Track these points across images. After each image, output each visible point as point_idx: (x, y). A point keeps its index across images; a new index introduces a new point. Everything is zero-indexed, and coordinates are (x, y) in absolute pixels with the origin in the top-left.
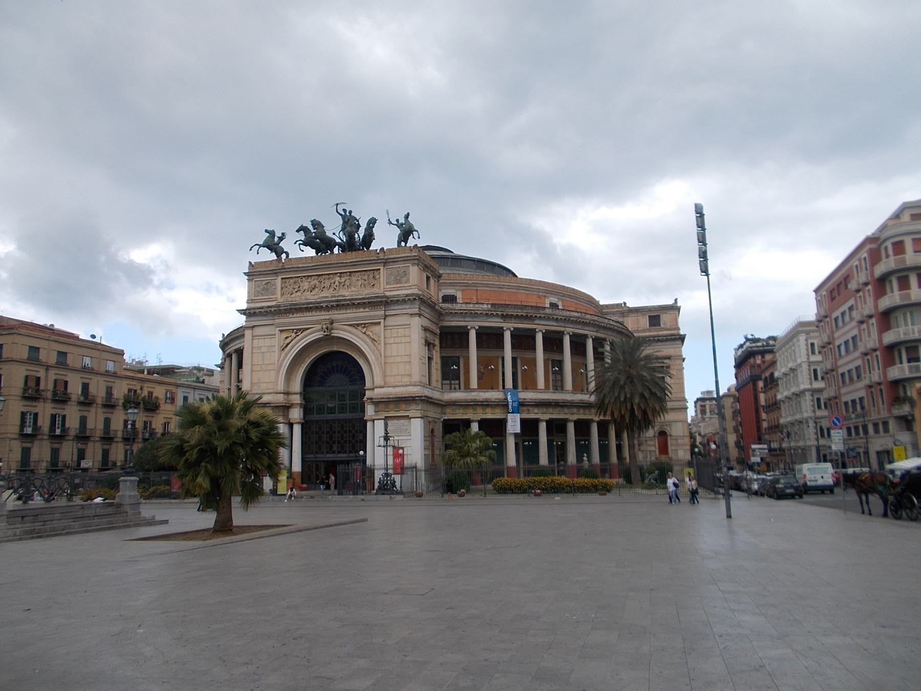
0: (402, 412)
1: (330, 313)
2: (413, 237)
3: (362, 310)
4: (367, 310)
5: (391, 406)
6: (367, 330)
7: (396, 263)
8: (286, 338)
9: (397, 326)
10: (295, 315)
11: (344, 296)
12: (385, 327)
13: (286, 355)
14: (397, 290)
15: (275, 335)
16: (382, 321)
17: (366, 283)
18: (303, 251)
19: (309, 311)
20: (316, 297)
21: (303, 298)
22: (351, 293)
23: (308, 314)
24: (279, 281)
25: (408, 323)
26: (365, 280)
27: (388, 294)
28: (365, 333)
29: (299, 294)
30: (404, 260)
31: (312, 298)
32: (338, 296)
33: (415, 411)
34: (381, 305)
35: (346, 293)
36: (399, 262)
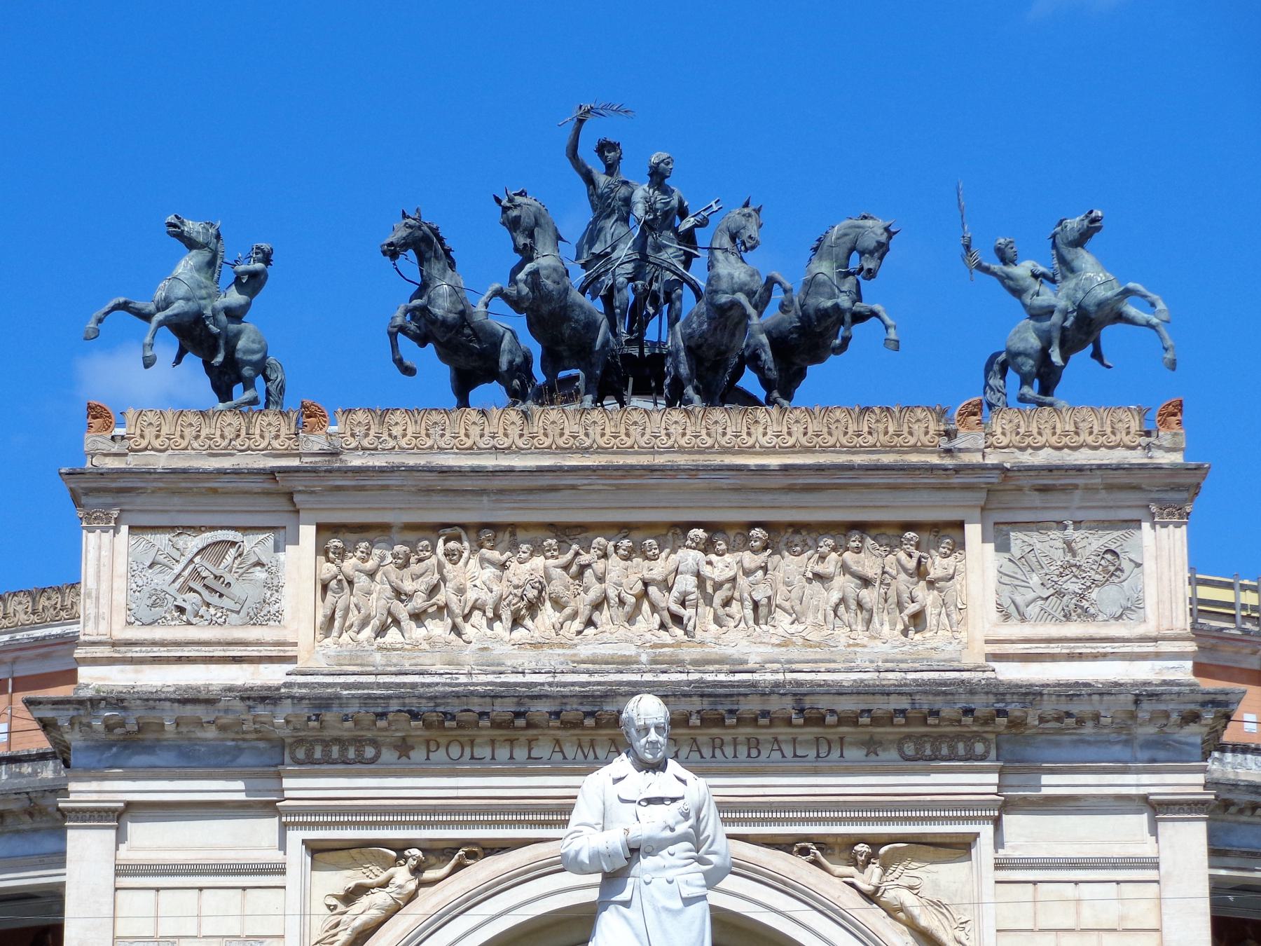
2: (1097, 355)
3: (853, 753)
7: (1055, 499)
8: (351, 896)
10: (418, 755)
11: (737, 665)
12: (999, 866)
14: (1071, 657)
15: (280, 870)
16: (986, 831)
17: (868, 595)
18: (408, 371)
19: (512, 742)
20: (552, 658)
21: (468, 655)
22: (782, 653)
25: (1146, 849)
26: (866, 582)
27: (1010, 673)
29: (437, 629)
30: (1110, 488)
31: (526, 659)
32: (695, 663)
34: (978, 736)
36: (1078, 494)
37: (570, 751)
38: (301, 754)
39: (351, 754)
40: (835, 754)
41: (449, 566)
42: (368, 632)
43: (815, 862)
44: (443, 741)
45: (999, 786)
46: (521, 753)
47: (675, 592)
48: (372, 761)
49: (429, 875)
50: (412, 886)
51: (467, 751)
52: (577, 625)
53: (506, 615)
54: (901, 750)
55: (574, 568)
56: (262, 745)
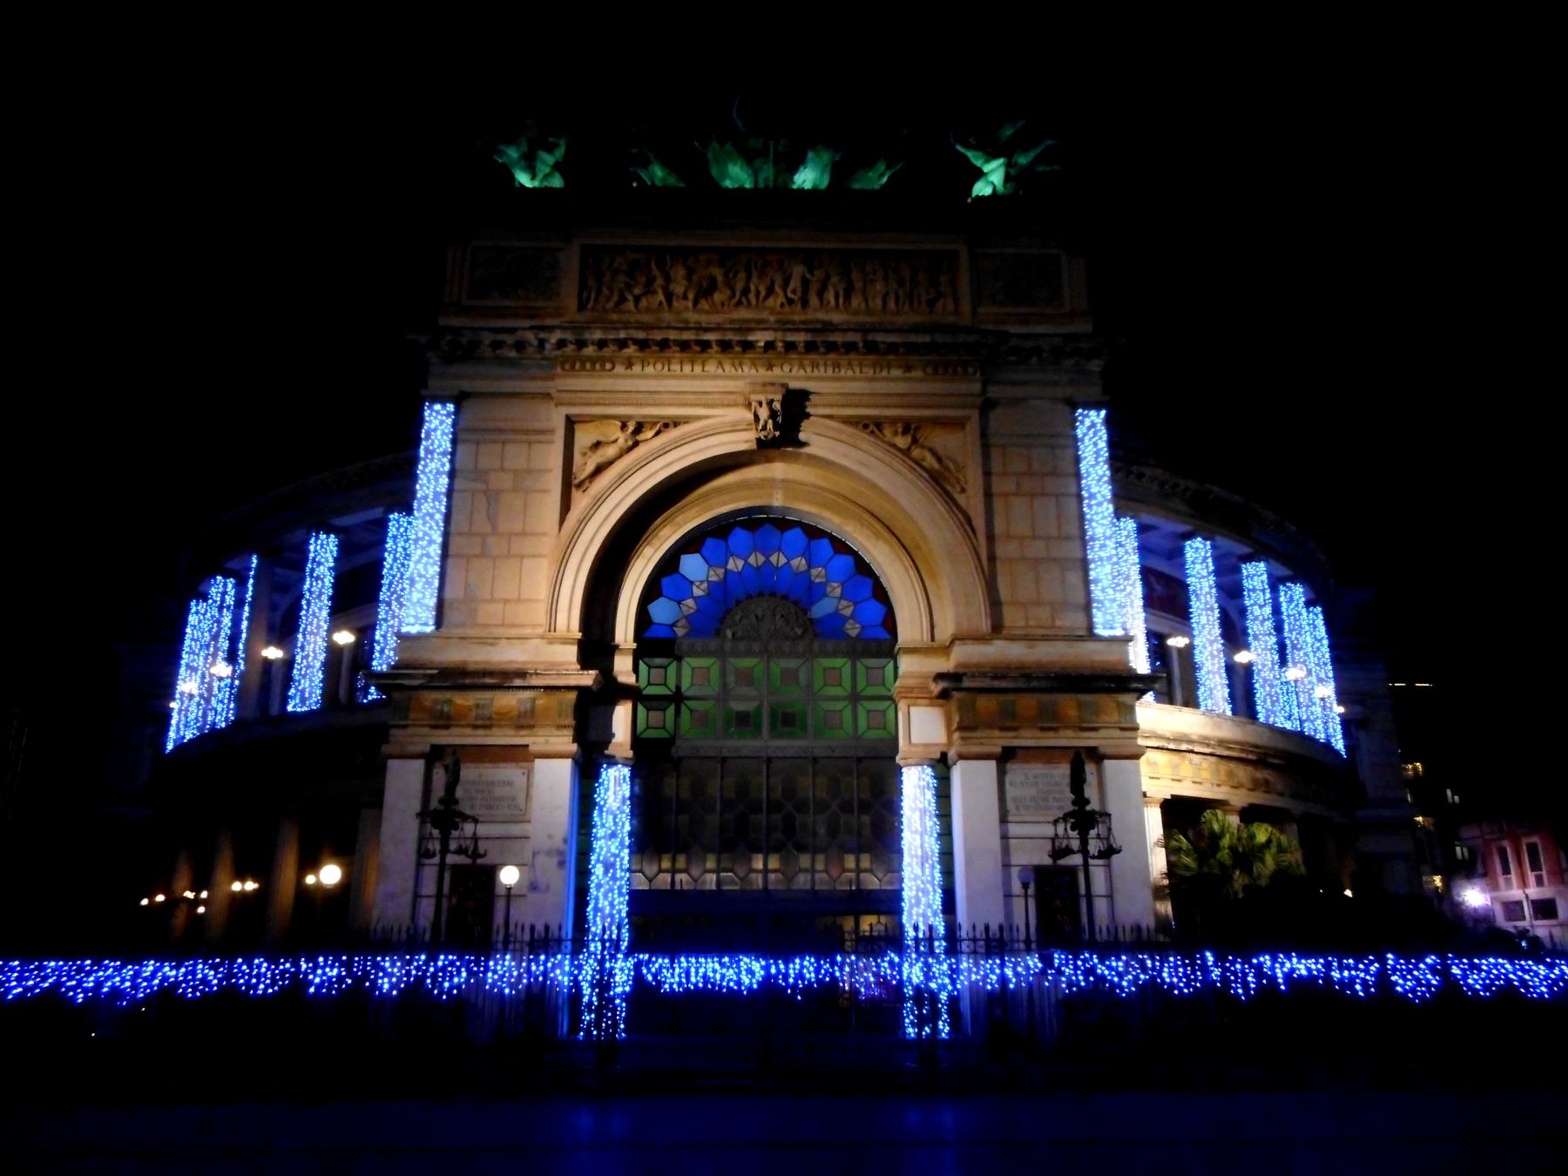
0: (1070, 733)
1: (777, 371)
3: (896, 373)
4: (917, 373)
5: (1027, 703)
6: (915, 441)
9: (1027, 436)
10: (637, 369)
13: (598, 502)
16: (975, 414)
22: (854, 319)
23: (687, 368)
24: (570, 260)
28: (906, 452)
33: (1118, 733)
35: (837, 318)
37: (727, 368)
38: (567, 366)
39: (598, 366)
40: (885, 373)
41: (656, 272)
42: (611, 305)
43: (872, 432)
44: (652, 361)
45: (984, 391)
46: (698, 369)
47: (792, 285)
48: (610, 370)
49: (640, 437)
50: (630, 443)
51: (666, 368)
52: (734, 301)
53: (691, 296)
54: (924, 371)
55: (731, 275)
56: (544, 362)
